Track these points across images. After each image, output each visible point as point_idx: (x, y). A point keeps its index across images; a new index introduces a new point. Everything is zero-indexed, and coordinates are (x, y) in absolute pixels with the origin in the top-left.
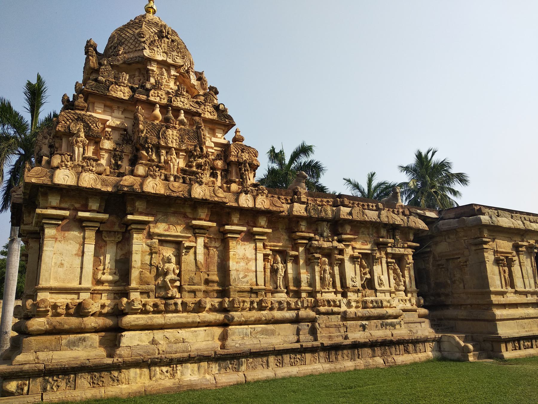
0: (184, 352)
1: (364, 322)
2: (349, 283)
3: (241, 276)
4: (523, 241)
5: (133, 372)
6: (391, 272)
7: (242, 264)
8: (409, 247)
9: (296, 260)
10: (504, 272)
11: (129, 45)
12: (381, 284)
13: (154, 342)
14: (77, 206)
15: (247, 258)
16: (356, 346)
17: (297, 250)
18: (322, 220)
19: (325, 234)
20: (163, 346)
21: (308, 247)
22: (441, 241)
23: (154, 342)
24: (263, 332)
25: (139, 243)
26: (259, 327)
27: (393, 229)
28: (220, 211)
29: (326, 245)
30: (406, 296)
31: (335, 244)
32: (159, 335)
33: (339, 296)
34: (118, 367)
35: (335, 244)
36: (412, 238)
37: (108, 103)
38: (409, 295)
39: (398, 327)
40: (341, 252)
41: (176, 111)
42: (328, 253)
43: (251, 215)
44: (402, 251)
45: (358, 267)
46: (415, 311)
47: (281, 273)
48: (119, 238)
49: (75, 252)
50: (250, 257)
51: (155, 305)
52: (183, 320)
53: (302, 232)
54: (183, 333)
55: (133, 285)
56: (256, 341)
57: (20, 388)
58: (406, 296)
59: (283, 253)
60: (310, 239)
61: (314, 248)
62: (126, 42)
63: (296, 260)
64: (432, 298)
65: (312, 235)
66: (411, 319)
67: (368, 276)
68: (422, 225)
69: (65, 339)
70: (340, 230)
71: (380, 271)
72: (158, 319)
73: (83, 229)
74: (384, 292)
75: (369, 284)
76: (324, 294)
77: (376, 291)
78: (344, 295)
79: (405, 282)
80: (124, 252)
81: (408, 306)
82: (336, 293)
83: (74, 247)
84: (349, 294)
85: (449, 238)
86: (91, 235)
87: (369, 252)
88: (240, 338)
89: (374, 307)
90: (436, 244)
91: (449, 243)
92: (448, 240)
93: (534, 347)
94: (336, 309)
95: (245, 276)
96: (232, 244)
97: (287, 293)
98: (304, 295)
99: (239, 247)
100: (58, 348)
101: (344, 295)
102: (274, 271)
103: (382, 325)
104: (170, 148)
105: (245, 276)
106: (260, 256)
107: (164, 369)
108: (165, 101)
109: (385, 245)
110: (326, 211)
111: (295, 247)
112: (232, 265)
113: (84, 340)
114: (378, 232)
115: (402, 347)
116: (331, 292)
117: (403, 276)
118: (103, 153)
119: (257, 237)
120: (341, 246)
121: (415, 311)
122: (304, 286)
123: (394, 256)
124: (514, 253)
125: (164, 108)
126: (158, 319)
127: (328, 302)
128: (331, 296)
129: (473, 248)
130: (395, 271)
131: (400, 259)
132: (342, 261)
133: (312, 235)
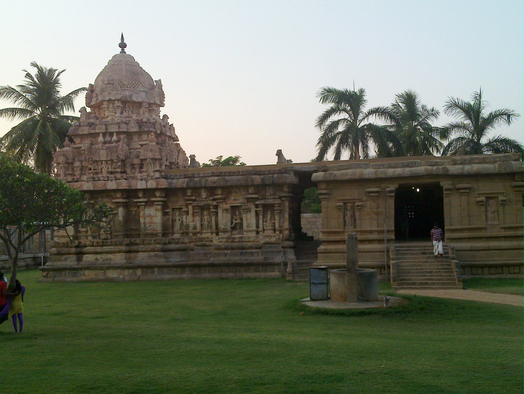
1: (226, 252)
2: (221, 226)
5: (87, 272)
9: (187, 213)
13: (97, 259)
15: (151, 216)
16: (212, 265)
23: (97, 259)
24: (155, 256)
26: (152, 254)
30: (275, 233)
32: (99, 256)
33: (214, 235)
34: (81, 269)
35: (210, 202)
40: (216, 207)
41: (111, 134)
50: (153, 215)
51: (98, 243)
52: (110, 250)
54: (110, 256)
57: (47, 274)
72: (99, 249)
76: (203, 234)
78: (217, 234)
82: (212, 233)
84: (220, 234)
87: (240, 205)
88: (142, 258)
95: (150, 226)
98: (191, 235)
100: (58, 261)
101: (217, 234)
105: (150, 226)
107: (101, 272)
108: (104, 131)
113: (70, 258)
116: (208, 233)
118: (75, 169)
119: (155, 203)
120: (215, 203)
122: (191, 229)
125: (104, 134)
126: (99, 249)
128: (209, 235)
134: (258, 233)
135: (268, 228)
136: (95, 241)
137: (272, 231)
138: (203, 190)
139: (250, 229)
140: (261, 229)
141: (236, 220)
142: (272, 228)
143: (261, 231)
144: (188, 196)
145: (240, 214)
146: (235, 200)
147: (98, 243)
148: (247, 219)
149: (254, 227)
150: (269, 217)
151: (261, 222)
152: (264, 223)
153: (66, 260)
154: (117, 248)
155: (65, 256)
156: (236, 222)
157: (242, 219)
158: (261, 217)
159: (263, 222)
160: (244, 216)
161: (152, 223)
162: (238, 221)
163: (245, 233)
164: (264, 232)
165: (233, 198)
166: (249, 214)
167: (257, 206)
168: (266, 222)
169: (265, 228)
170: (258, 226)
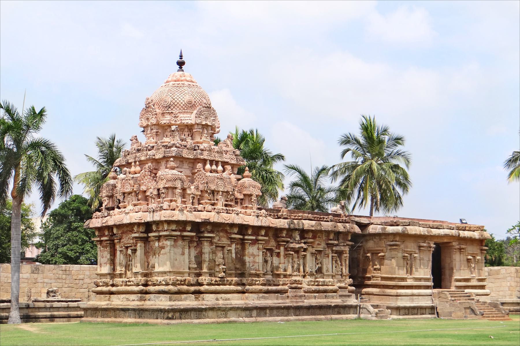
0: (231, 305)
3: (251, 265)
4: (424, 243)
6: (334, 262)
7: (252, 258)
8: (347, 245)
9: (278, 255)
10: (407, 264)
11: (180, 107)
12: (327, 271)
14: (181, 228)
17: (279, 249)
18: (296, 229)
19: (297, 239)
20: (221, 302)
21: (286, 247)
22: (370, 240)
24: (262, 297)
25: (207, 248)
26: (261, 295)
27: (338, 234)
28: (243, 228)
29: (297, 246)
31: (303, 245)
35: (303, 245)
36: (350, 238)
37: (181, 160)
38: (344, 277)
39: (335, 297)
42: (297, 251)
43: (257, 229)
44: (342, 248)
45: (314, 259)
46: (346, 288)
47: (269, 262)
48: (195, 244)
49: (181, 253)
50: (255, 254)
51: (216, 281)
53: (283, 237)
55: (205, 270)
56: (260, 302)
58: (342, 277)
59: (271, 250)
60: (288, 242)
61: (290, 248)
62: (178, 105)
63: (278, 255)
64: (360, 280)
65: (289, 239)
66: (344, 293)
67: (320, 265)
68: (357, 230)
69: (184, 296)
70: (306, 236)
71: (327, 264)
73: (183, 240)
74: (328, 275)
75: (319, 271)
77: (323, 273)
79: (342, 269)
80: (197, 252)
81: (343, 285)
83: (180, 250)
85: (375, 238)
86: (186, 243)
89: (322, 285)
90: (367, 241)
91: (375, 241)
92: (374, 240)
93: (419, 314)
94: (299, 286)
95: (253, 265)
96: (247, 246)
97: (272, 275)
99: (250, 248)
100: (181, 300)
102: (266, 261)
103: (326, 296)
104: (219, 191)
105: (253, 265)
106: (261, 253)
109: (333, 245)
110: (298, 224)
111: (278, 247)
112: (247, 259)
114: (328, 236)
115: (336, 310)
117: (341, 265)
119: (260, 242)
121: (346, 288)
123: (337, 252)
124: (417, 251)
127: (295, 281)
129: (389, 248)
130: (336, 261)
131: (340, 253)
132: (305, 256)
133: (289, 239)
136: (214, 279)
138: (297, 232)
144: (283, 237)
146: (319, 244)
147: (216, 281)
153: (185, 299)
154: (232, 288)
155: (185, 295)
161: (254, 262)
165: (317, 242)
167: (332, 251)
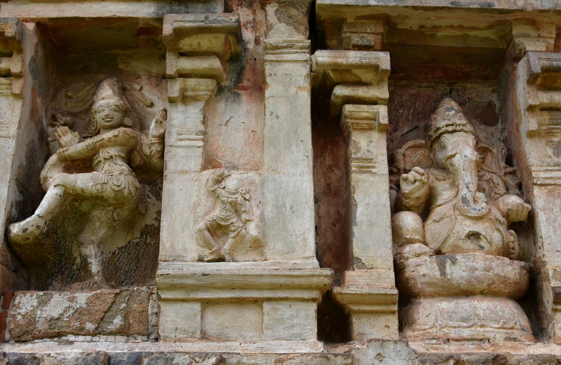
30: (539, 330)
134: (335, 323)
135: (458, 272)
137: (509, 310)
139: (243, 265)
140: (371, 277)
141: (84, 163)
142: (511, 270)
143: (374, 303)
145: (132, 115)
148: (209, 162)
149: (296, 248)
150: (461, 148)
151: (371, 195)
152: (409, 220)
156: (82, 181)
157: (149, 173)
158: (369, 147)
159: (397, 207)
160: (184, 121)
162: (112, 176)
163: (174, 317)
164: (404, 323)
166: (237, 120)
168: (425, 209)
169: (422, 268)
170: (336, 248)
